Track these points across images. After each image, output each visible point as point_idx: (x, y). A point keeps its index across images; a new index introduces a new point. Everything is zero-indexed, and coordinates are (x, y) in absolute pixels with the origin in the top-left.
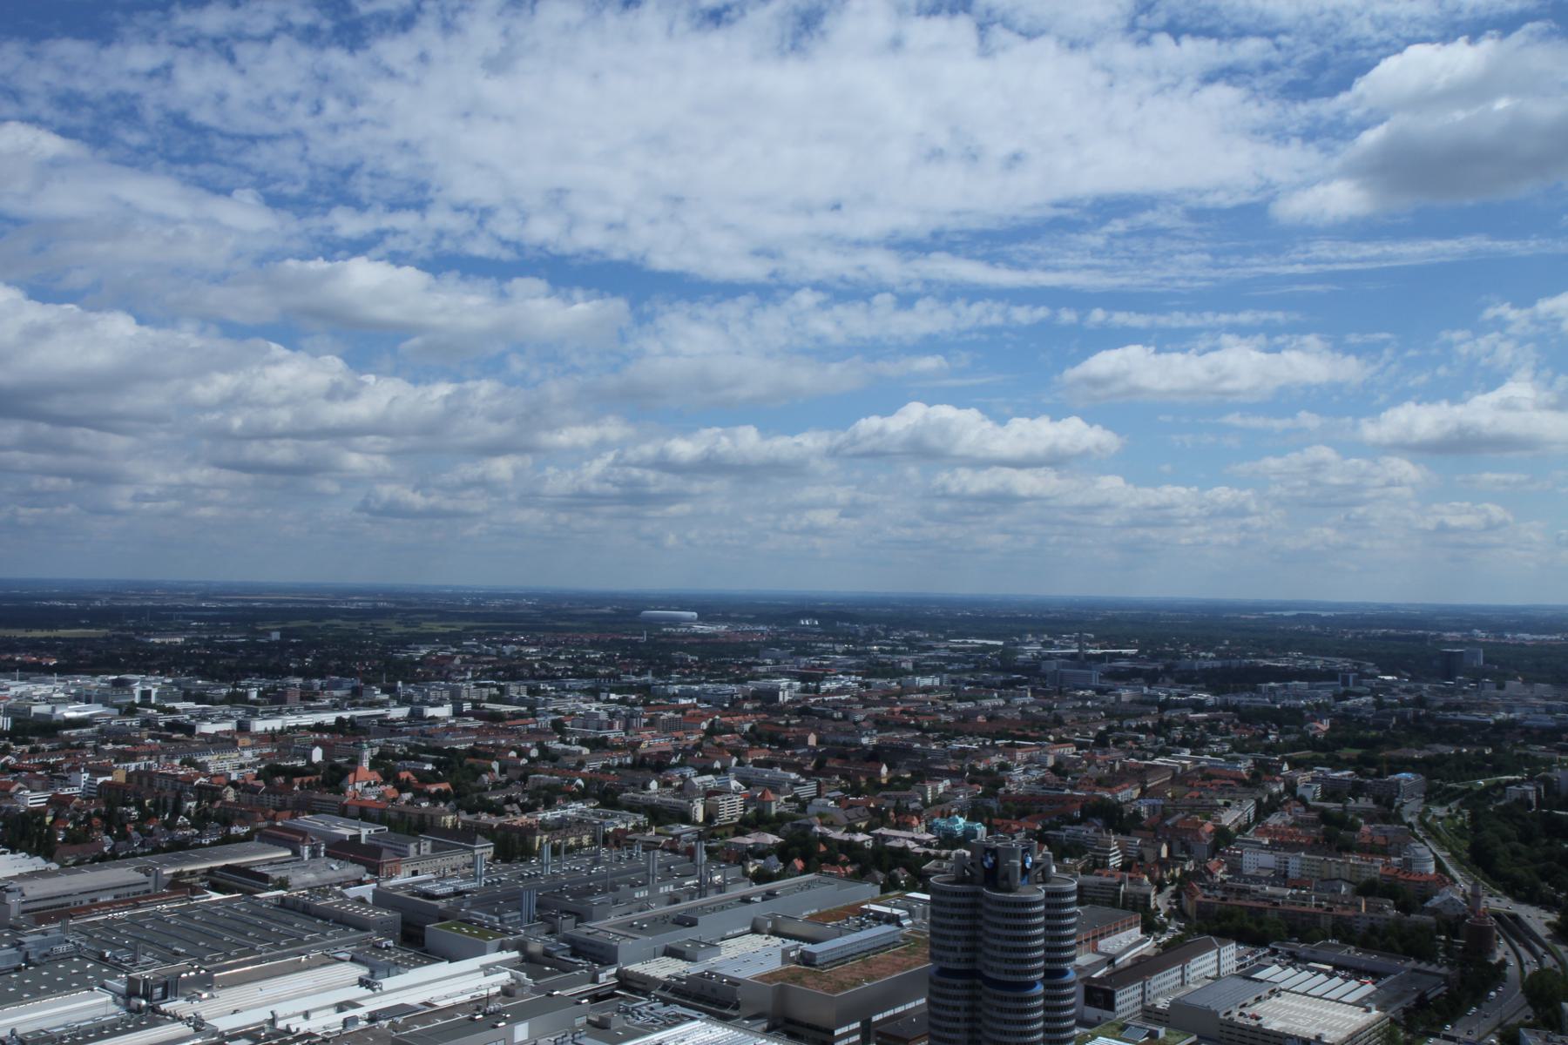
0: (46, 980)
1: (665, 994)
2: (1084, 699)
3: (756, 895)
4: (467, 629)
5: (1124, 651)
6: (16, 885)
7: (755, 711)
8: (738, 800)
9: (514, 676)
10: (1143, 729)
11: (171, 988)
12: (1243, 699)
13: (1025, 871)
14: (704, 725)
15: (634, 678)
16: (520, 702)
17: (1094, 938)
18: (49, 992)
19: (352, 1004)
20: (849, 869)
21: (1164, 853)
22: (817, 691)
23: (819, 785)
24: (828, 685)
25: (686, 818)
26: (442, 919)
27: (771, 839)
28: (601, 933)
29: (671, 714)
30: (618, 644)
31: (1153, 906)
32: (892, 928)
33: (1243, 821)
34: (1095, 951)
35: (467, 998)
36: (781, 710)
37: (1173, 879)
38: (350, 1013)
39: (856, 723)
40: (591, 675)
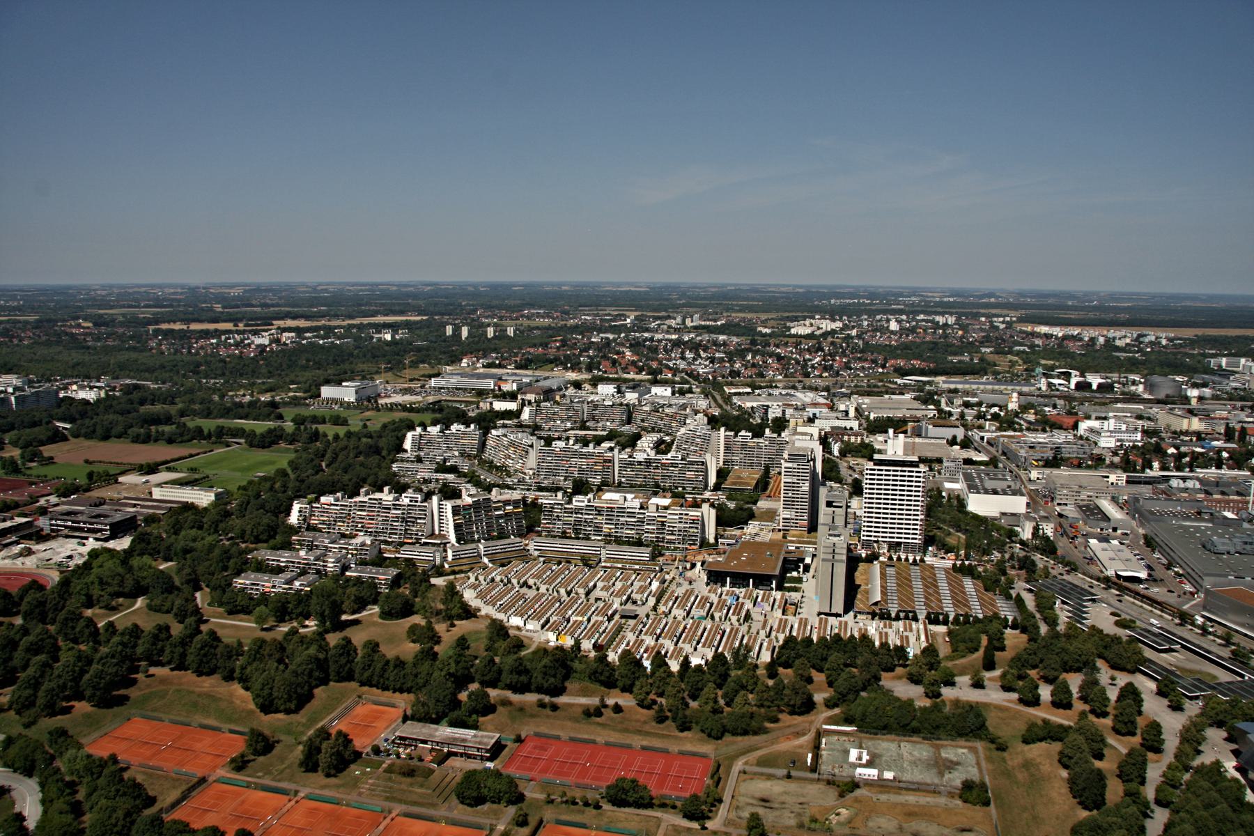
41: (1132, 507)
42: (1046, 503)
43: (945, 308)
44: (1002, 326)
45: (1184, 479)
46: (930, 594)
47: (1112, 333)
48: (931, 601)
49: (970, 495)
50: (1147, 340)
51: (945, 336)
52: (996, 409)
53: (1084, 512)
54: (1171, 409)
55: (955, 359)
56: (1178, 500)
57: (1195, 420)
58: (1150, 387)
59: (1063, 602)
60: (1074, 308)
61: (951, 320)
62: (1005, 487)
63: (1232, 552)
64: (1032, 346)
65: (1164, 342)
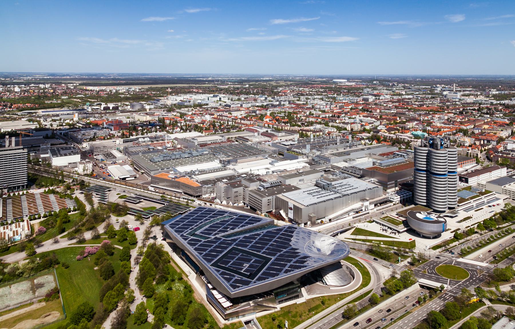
0: (203, 159)
1: (343, 171)
2: (456, 102)
3: (365, 148)
4: (291, 84)
5: (467, 89)
6: (196, 138)
7: (363, 104)
8: (359, 125)
9: (302, 95)
10: (474, 110)
11: (229, 162)
12: (506, 102)
13: (442, 145)
14: (350, 107)
15: (331, 96)
16: (304, 101)
17: (461, 164)
18: (204, 161)
19: (268, 169)
20: (390, 143)
21: (482, 142)
22: (379, 99)
23: (381, 122)
24: (381, 98)
25: (345, 129)
26: (288, 150)
27: (368, 135)
28: (326, 156)
29: (341, 104)
30: (327, 88)
31: (479, 157)
32: (402, 158)
33: (507, 135)
34: (461, 167)
35: (294, 169)
36: (369, 104)
37: (485, 150)
38: (268, 170)
39: (390, 107)
40: (322, 95)
41: (126, 151)
42: (90, 155)
43: (44, 81)
44: (72, 88)
45: (144, 138)
46: (31, 207)
47: (118, 88)
48: (32, 210)
49: (53, 158)
50: (131, 90)
51: (44, 92)
52: (68, 121)
53: (106, 156)
54: (140, 114)
55: (49, 102)
56: (142, 146)
57: (148, 116)
58: (132, 106)
59: (97, 194)
60: (103, 79)
61: (47, 86)
62: (70, 152)
63: (160, 161)
64: (85, 95)
65: (138, 90)
